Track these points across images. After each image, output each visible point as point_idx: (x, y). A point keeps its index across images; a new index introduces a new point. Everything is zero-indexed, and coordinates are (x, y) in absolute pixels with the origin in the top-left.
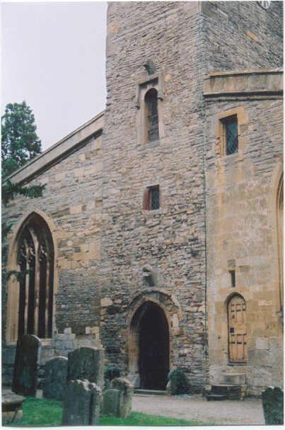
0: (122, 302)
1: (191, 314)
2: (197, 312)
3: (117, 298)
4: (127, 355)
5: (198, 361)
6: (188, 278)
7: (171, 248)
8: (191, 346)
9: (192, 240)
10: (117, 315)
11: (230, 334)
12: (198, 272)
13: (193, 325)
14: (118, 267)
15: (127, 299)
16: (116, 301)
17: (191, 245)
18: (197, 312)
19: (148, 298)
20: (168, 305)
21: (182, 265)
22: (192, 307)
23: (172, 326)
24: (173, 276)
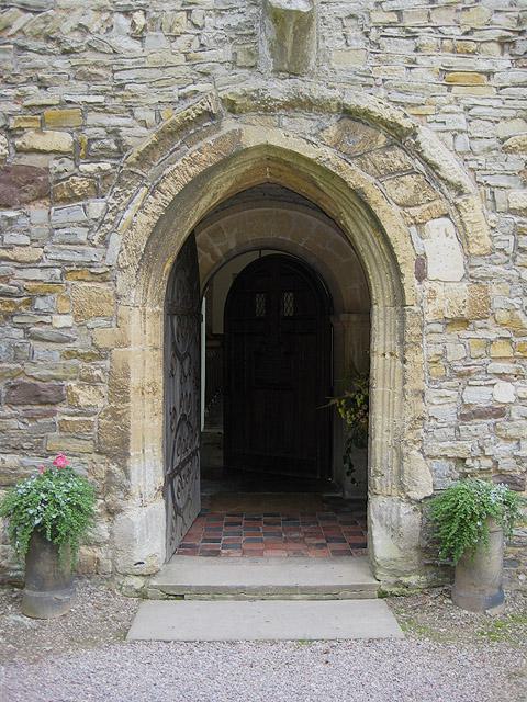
0: (77, 145)
4: (115, 415)
6: (516, 58)
10: (38, 212)
15: (114, 132)
16: (32, 139)
19: (257, 134)
20: (395, 173)
23: (421, 275)
24: (426, 38)
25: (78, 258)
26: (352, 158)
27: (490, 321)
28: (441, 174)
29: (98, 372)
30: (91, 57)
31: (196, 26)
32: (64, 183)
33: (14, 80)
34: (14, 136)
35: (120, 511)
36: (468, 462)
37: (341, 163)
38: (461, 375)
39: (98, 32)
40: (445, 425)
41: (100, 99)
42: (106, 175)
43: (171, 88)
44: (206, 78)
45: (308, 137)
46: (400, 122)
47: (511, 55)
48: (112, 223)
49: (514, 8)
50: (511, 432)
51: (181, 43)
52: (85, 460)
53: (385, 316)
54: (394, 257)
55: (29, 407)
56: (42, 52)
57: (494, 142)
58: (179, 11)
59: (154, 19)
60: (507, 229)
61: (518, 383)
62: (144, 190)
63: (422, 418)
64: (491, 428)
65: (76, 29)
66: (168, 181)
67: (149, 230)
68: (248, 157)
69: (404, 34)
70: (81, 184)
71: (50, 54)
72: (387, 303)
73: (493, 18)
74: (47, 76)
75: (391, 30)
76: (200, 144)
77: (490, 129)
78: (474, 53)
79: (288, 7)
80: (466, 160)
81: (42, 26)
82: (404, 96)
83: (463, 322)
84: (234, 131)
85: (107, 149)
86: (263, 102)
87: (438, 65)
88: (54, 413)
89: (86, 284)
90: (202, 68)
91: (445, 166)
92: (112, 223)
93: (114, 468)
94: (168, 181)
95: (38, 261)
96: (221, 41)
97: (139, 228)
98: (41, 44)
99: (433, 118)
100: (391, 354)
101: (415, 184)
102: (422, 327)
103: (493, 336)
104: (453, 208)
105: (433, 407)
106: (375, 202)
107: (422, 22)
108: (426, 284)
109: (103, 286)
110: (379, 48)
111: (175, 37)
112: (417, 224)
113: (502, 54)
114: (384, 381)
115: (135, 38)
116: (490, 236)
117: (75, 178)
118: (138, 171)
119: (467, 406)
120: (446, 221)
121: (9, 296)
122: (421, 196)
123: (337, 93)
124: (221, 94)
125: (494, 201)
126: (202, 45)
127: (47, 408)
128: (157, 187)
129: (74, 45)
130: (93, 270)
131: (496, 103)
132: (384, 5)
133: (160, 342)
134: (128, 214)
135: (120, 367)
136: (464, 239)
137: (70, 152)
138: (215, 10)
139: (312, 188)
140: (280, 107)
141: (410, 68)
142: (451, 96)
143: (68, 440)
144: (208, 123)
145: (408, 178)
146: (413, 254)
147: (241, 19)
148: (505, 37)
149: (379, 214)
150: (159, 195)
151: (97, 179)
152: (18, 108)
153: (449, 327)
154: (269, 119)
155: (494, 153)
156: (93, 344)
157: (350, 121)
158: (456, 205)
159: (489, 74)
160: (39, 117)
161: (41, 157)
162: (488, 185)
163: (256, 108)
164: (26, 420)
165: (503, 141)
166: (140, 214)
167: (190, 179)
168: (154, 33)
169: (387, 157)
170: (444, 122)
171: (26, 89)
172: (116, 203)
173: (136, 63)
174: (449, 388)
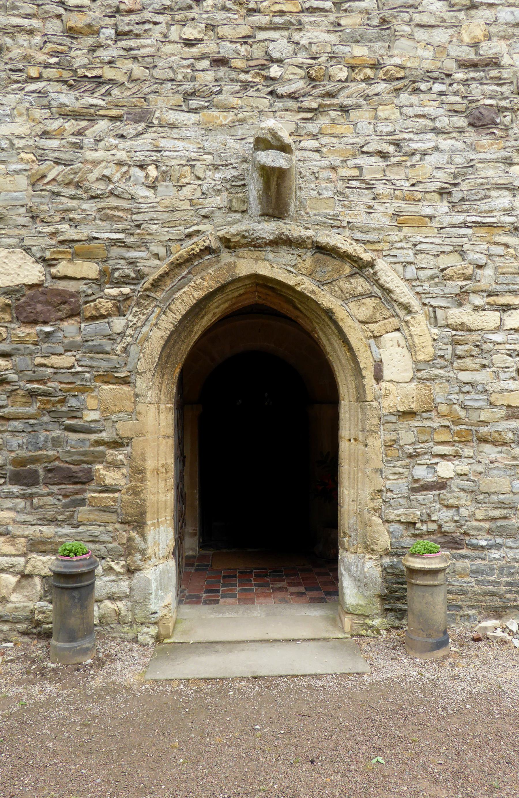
0: (103, 273)
2: (498, 329)
3: (76, 255)
4: (135, 492)
5: (500, 505)
6: (453, 205)
7: (367, 80)
8: (468, 451)
9: (474, 66)
12: (498, 187)
13: (480, 376)
14: (71, 125)
17: (466, 83)
18: (498, 329)
20: (358, 297)
21: (424, 154)
22: (476, 308)
23: (378, 378)
24: (381, 188)
25: (104, 364)
26: (323, 285)
27: (433, 414)
28: (395, 297)
29: (121, 457)
30: (113, 202)
31: (199, 178)
32: (92, 304)
33: (49, 219)
34: (51, 265)
35: (138, 569)
36: (418, 525)
37: (315, 288)
38: (410, 456)
39: (118, 182)
40: (399, 496)
41: (121, 236)
42: (127, 298)
43: (180, 228)
44: (206, 220)
45: (289, 268)
46: (362, 256)
47: (449, 202)
48: (132, 336)
49: (450, 166)
50: (452, 501)
51: (186, 191)
52: (110, 528)
53: (350, 409)
54: (356, 363)
55: (62, 486)
56: (73, 197)
57: (435, 271)
58: (184, 166)
59: (164, 172)
60: (446, 340)
61: (456, 462)
62: (157, 310)
63: (380, 491)
64: (436, 498)
65: (101, 179)
66: (177, 303)
67: (162, 342)
68: (239, 285)
69: (364, 186)
70: (106, 305)
71: (79, 199)
72: (352, 399)
73: (434, 174)
74: (78, 217)
75: (353, 182)
76: (203, 273)
77: (433, 261)
78: (419, 200)
79: (273, 164)
80: (413, 286)
81: (72, 176)
82: (362, 235)
83: (410, 414)
84: (230, 263)
85: (127, 276)
86: (253, 240)
87: (391, 211)
88: (85, 491)
89: (111, 386)
90: (204, 212)
91: (398, 291)
92: (132, 336)
93: (134, 534)
94: (177, 303)
95: (71, 367)
96: (218, 190)
97: (154, 341)
98: (72, 191)
99: (388, 252)
100: (355, 440)
101: (374, 305)
102: (380, 419)
103: (436, 425)
104: (403, 324)
105: (388, 482)
106: (342, 320)
107: (378, 176)
108: (383, 384)
109: (125, 388)
110: (344, 197)
111: (181, 186)
112: (375, 337)
113: (442, 202)
114: (350, 461)
115: (149, 187)
116: (433, 346)
117: (100, 299)
118: (152, 294)
119: (416, 481)
120: (397, 334)
121: (46, 396)
122: (378, 315)
123: (311, 233)
124: (220, 234)
125: (436, 318)
126: (203, 194)
127: (79, 487)
128: (168, 307)
129: (99, 192)
130: (116, 375)
131: (438, 241)
132: (348, 163)
133: (171, 431)
134: (145, 329)
135: (139, 453)
136: (412, 348)
137: (97, 279)
138: (213, 165)
139: (291, 308)
140: (266, 244)
141: (369, 213)
142: (401, 235)
143: (96, 513)
144: (208, 257)
145: (368, 300)
146: (372, 361)
147: (235, 173)
148: (444, 188)
149: (346, 330)
150: (170, 314)
151: (119, 301)
152: (53, 242)
153: (401, 419)
154: (257, 254)
155: (436, 280)
156: (117, 434)
157: (322, 255)
158: (406, 322)
159: (431, 217)
160: (71, 250)
161: (72, 283)
162: (431, 306)
163: (247, 245)
164: (60, 497)
165: (442, 270)
166: (154, 329)
167: (195, 302)
168: (165, 183)
169: (351, 284)
170: (396, 256)
171: (59, 227)
172: (135, 320)
173: (150, 207)
174: (402, 467)
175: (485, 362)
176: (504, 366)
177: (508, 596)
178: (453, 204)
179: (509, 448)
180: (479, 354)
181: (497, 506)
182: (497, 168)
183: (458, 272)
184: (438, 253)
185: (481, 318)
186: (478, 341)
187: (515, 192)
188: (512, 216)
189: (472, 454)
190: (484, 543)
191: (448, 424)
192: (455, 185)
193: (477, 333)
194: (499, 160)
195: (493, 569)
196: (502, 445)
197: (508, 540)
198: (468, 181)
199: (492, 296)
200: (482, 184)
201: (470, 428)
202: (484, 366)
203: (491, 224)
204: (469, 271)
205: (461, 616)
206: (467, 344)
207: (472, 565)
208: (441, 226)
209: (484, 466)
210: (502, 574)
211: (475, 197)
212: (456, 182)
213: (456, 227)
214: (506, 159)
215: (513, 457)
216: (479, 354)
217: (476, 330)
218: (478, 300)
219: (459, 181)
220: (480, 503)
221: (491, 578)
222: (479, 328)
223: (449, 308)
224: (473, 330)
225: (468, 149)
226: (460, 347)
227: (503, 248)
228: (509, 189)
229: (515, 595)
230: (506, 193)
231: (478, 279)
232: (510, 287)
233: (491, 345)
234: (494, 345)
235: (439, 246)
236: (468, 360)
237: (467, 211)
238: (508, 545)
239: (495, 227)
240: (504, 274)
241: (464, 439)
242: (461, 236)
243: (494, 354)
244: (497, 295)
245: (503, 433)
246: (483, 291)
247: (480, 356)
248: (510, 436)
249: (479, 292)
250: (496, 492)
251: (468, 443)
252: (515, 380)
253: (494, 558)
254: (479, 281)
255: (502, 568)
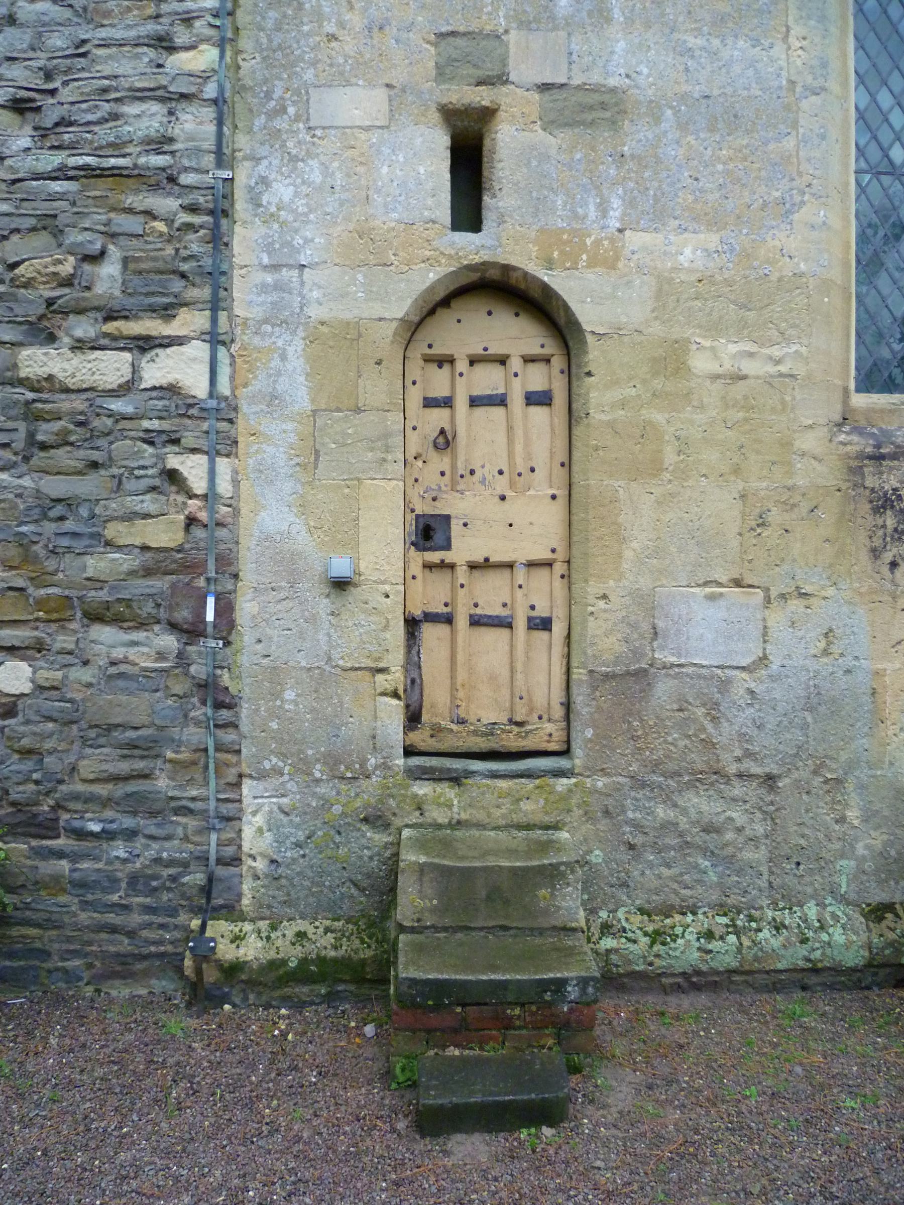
1: (67, 404)
6: (42, 133)
8: (64, 641)
11: (417, 558)
12: (140, 95)
22: (79, 346)
47: (36, 128)
60: (13, 412)
113: (21, 128)
175: (96, 456)
176: (136, 464)
177: (145, 933)
178: (43, 132)
179: (149, 634)
180: (86, 440)
181: (126, 752)
182: (137, 56)
183: (43, 271)
184: (6, 233)
185: (89, 366)
186: (81, 413)
187: (174, 104)
188: (165, 153)
189: (71, 646)
190: (96, 827)
191: (20, 583)
192: (53, 92)
193: (84, 396)
194: (142, 41)
195: (117, 881)
196: (137, 628)
197: (148, 822)
198: (76, 84)
199: (115, 319)
200: (105, 90)
201: (67, 593)
202: (95, 465)
203: (115, 172)
204: (67, 268)
205: (49, 971)
206: (60, 419)
207: (75, 870)
208: (13, 177)
209: (96, 671)
210: (134, 890)
211: (90, 117)
212: (50, 86)
213: (45, 179)
214: (160, 39)
215: (158, 653)
216: (86, 440)
217: (79, 391)
218: (84, 328)
219: (57, 84)
220: (91, 746)
221: (110, 897)
222: (84, 386)
223: (21, 344)
224: (73, 391)
225: (75, 19)
226: (44, 426)
227: (141, 219)
228: (162, 100)
229: (161, 932)
230: (155, 107)
231: (84, 284)
232: (152, 300)
233: (109, 422)
234: (117, 421)
235: (7, 219)
236: (61, 452)
237: (72, 147)
238: (146, 832)
239: (128, 176)
240: (140, 273)
241: (55, 616)
242: (52, 198)
243: (117, 440)
244: (126, 318)
245: (135, 605)
246: (97, 309)
247: (86, 444)
248: (150, 610)
249: (87, 310)
250: (119, 725)
251: (67, 624)
252: (160, 493)
253: (117, 858)
254: (88, 288)
255: (133, 879)
